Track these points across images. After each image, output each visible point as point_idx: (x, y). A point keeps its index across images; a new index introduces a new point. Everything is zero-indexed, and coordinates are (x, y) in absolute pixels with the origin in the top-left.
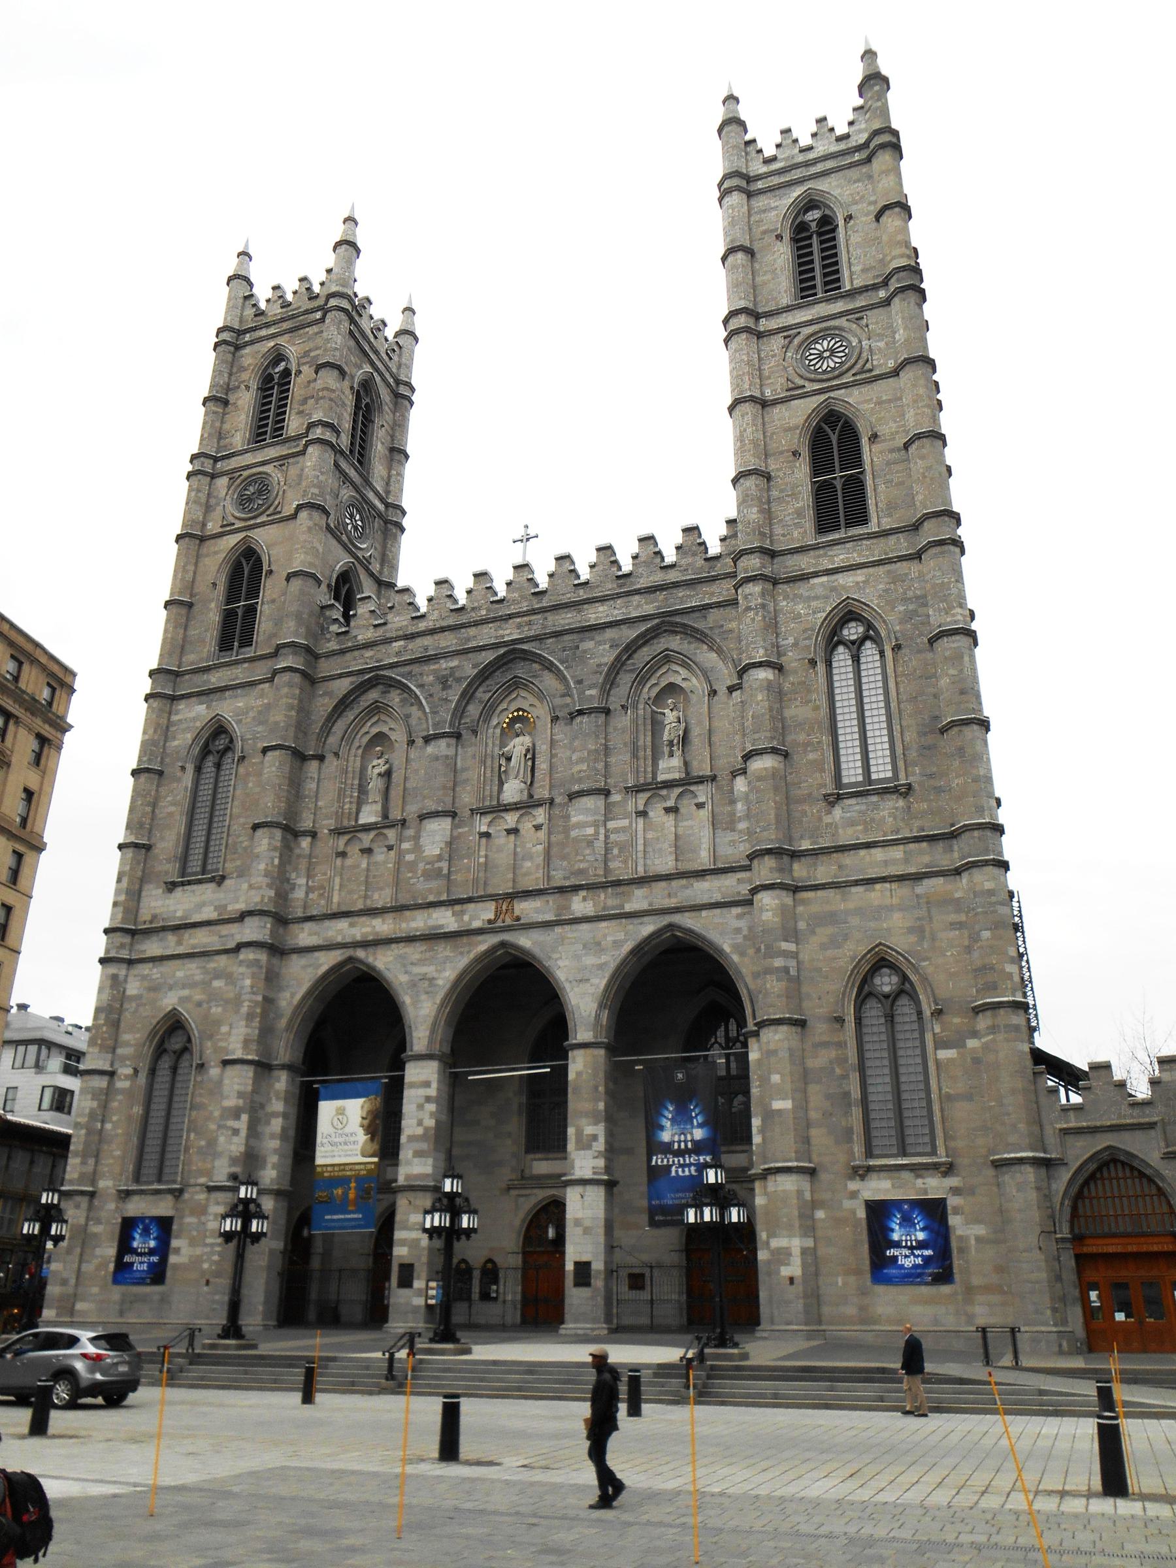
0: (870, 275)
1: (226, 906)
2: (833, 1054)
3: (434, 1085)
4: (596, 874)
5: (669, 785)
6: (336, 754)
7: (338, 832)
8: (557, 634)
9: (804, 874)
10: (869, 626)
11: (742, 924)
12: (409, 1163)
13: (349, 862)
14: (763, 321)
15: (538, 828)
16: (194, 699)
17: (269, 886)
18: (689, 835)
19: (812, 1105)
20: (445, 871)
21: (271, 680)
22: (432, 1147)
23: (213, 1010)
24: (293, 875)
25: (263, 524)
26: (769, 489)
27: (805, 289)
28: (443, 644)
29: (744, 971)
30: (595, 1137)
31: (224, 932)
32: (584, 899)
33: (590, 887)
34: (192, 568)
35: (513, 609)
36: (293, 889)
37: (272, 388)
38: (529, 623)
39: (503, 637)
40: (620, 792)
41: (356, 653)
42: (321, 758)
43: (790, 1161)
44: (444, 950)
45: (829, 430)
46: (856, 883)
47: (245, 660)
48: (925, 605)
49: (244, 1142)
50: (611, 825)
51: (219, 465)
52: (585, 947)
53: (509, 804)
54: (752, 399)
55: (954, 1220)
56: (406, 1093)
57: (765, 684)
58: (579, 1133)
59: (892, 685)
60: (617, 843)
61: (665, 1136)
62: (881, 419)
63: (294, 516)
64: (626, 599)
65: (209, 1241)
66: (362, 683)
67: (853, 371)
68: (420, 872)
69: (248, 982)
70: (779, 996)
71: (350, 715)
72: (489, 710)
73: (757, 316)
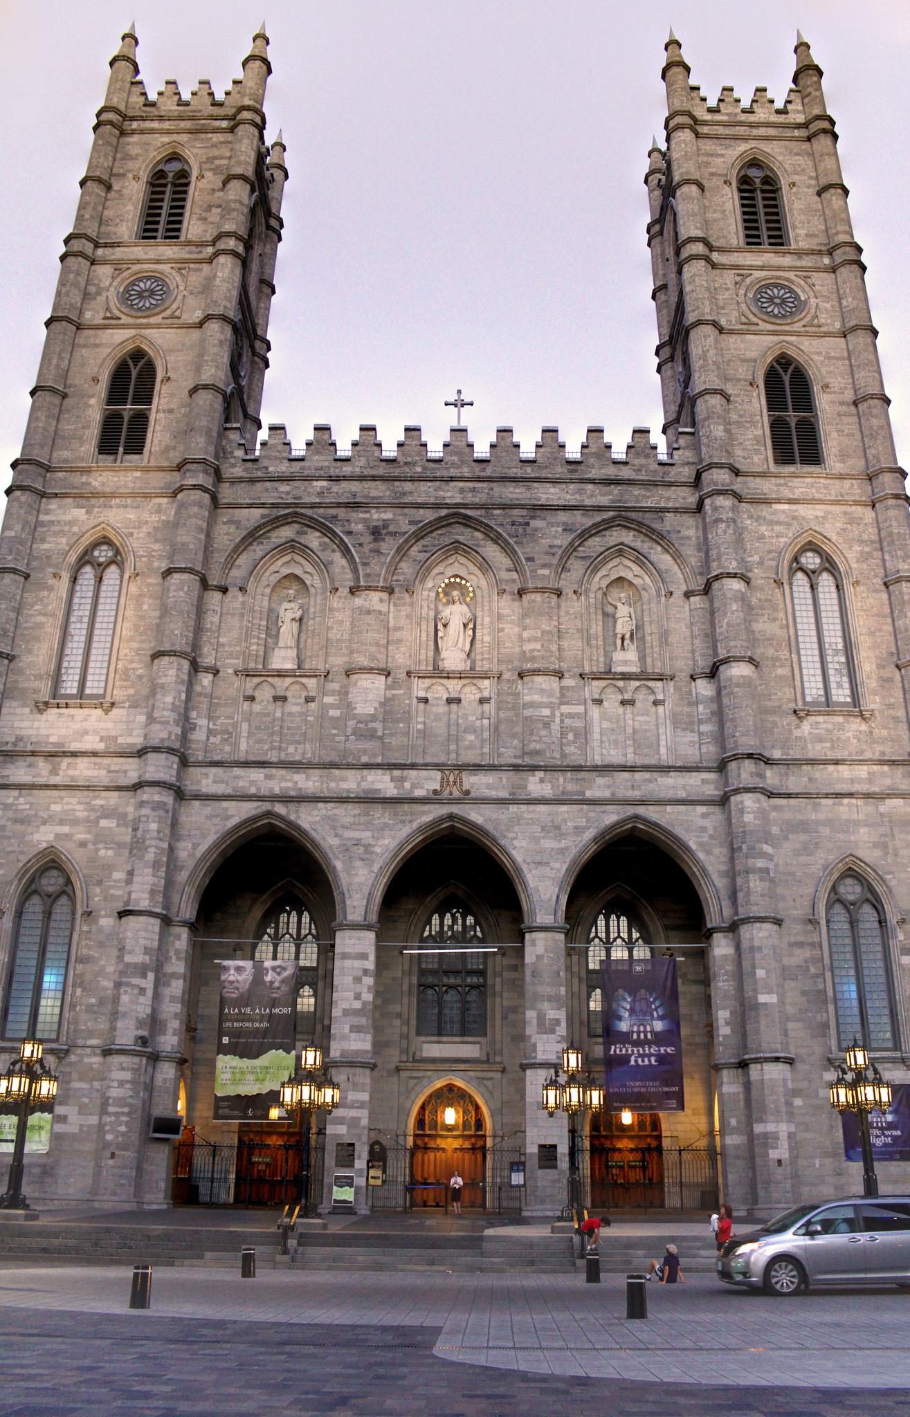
1: (116, 738)
2: (808, 953)
3: (372, 957)
4: (554, 757)
5: (626, 677)
6: (241, 589)
7: (248, 675)
8: (504, 507)
11: (707, 823)
12: (345, 1038)
13: (256, 708)
16: (70, 500)
17: (177, 723)
18: (646, 731)
19: (788, 1001)
21: (174, 494)
22: (370, 1022)
23: (102, 853)
24: (194, 714)
25: (158, 326)
26: (728, 411)
27: (752, 238)
28: (374, 493)
29: (710, 869)
30: (558, 1022)
31: (113, 768)
32: (542, 780)
34: (68, 356)
35: (453, 472)
36: (193, 728)
37: (165, 185)
38: (473, 490)
39: (444, 498)
40: (573, 676)
41: (268, 484)
42: (224, 590)
43: (777, 1051)
44: (380, 815)
45: (781, 371)
46: (827, 796)
47: (137, 469)
49: (150, 1002)
50: (565, 709)
51: (100, 252)
52: (543, 829)
53: (453, 671)
56: (338, 964)
57: (739, 595)
58: (541, 1018)
60: (572, 729)
61: (624, 1026)
62: (831, 372)
63: (201, 325)
65: (111, 1109)
66: (278, 518)
67: (803, 323)
68: (349, 731)
69: (154, 826)
70: (762, 895)
71: (258, 550)
72: (424, 570)
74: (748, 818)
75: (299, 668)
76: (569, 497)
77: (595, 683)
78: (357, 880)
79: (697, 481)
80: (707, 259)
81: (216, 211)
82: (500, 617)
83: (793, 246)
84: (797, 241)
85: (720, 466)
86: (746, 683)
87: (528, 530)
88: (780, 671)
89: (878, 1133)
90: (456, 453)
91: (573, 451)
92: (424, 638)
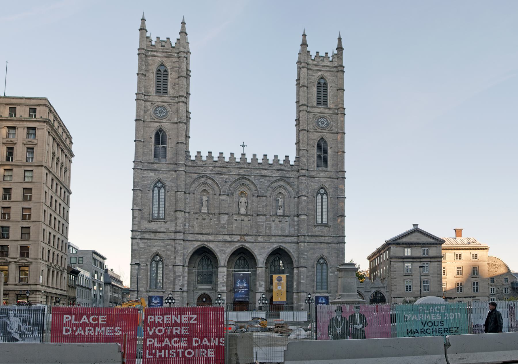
0: (334, 105)
4: (264, 233)
5: (280, 216)
7: (196, 213)
9: (309, 240)
10: (325, 191)
13: (199, 221)
14: (309, 108)
15: (249, 220)
28: (224, 171)
32: (261, 238)
33: (262, 236)
35: (242, 166)
39: (240, 173)
40: (269, 215)
44: (227, 245)
48: (337, 189)
50: (267, 222)
52: (261, 248)
54: (306, 130)
59: (329, 205)
60: (268, 227)
64: (271, 171)
67: (328, 129)
68: (220, 227)
72: (235, 190)
73: (308, 107)
74: (302, 247)
75: (208, 212)
76: (269, 173)
77: (273, 217)
78: (223, 258)
79: (298, 171)
80: (306, 111)
82: (253, 201)
83: (329, 107)
84: (330, 105)
85: (303, 169)
86: (304, 220)
88: (312, 217)
90: (243, 161)
91: (271, 162)
92: (236, 206)
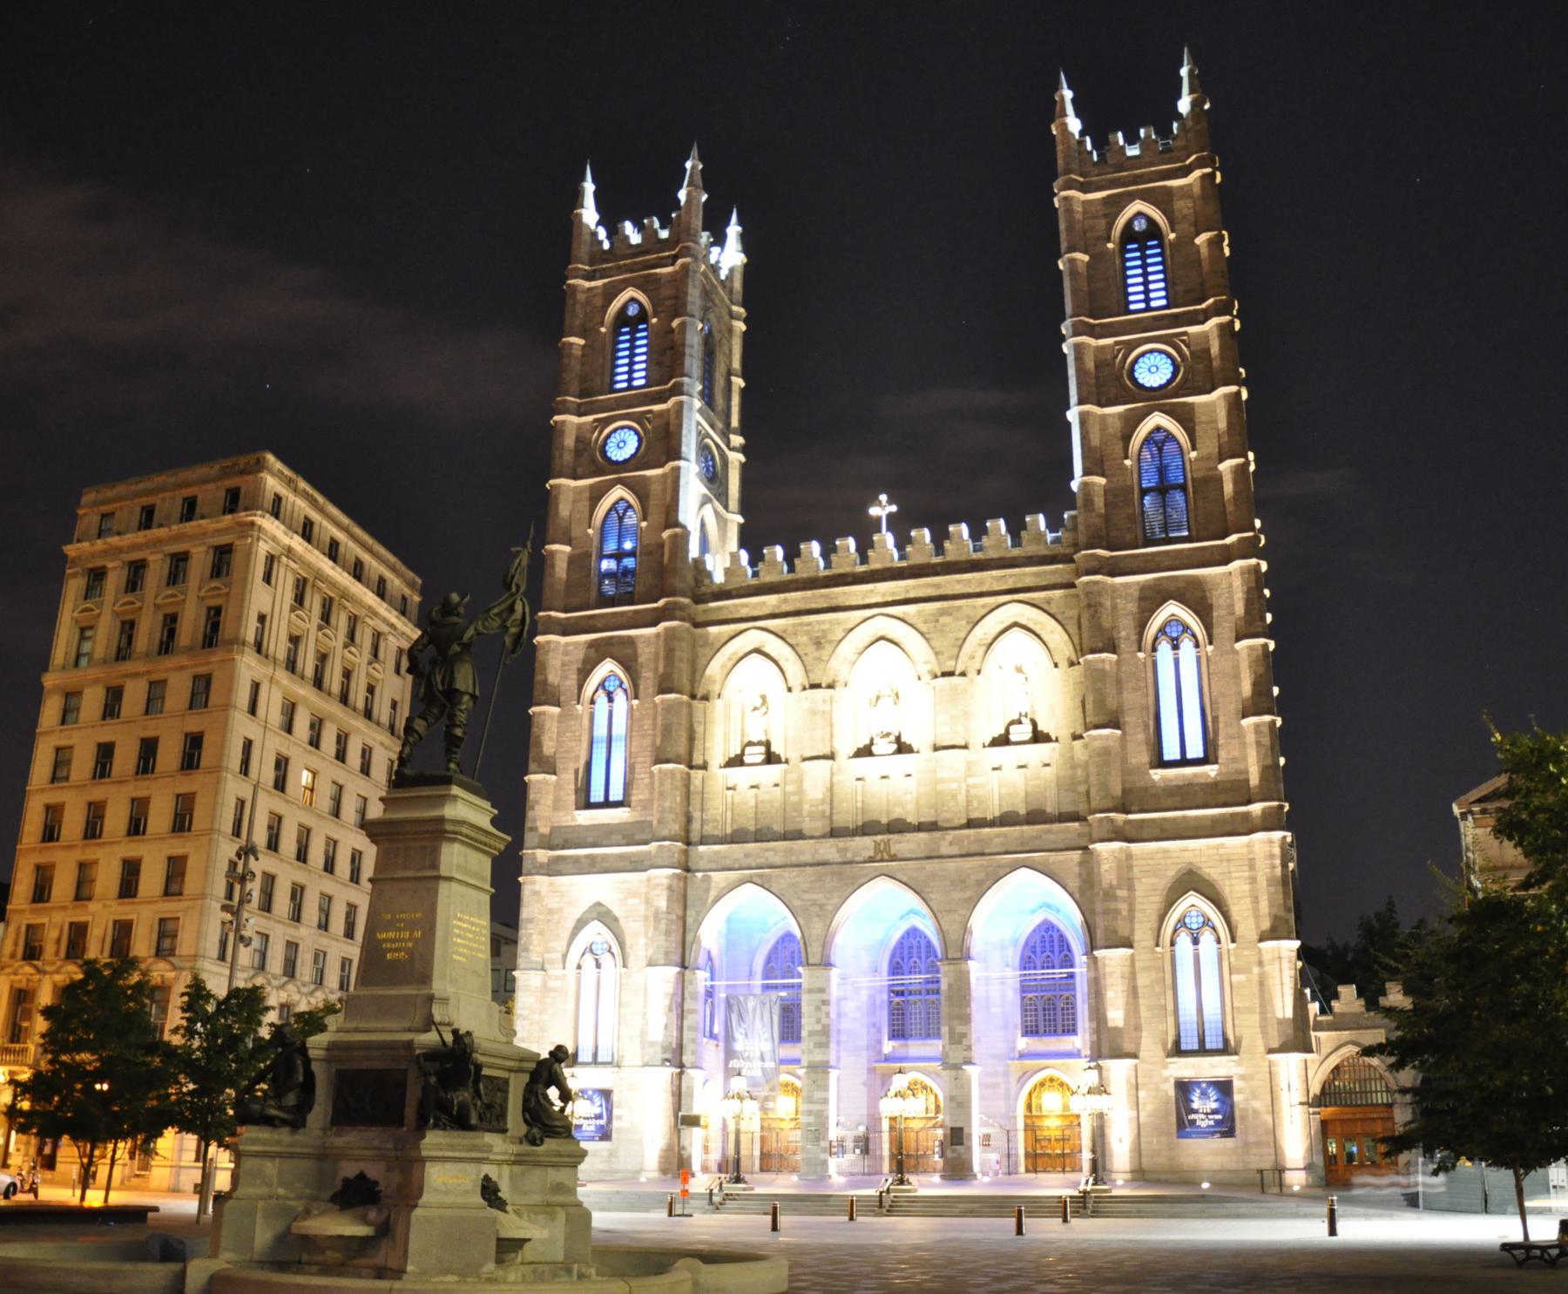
2: (1153, 976)
20: (828, 813)
32: (951, 844)
52: (952, 883)
55: (1237, 1097)
81: (668, 353)
87: (938, 625)
89: (1203, 1116)
